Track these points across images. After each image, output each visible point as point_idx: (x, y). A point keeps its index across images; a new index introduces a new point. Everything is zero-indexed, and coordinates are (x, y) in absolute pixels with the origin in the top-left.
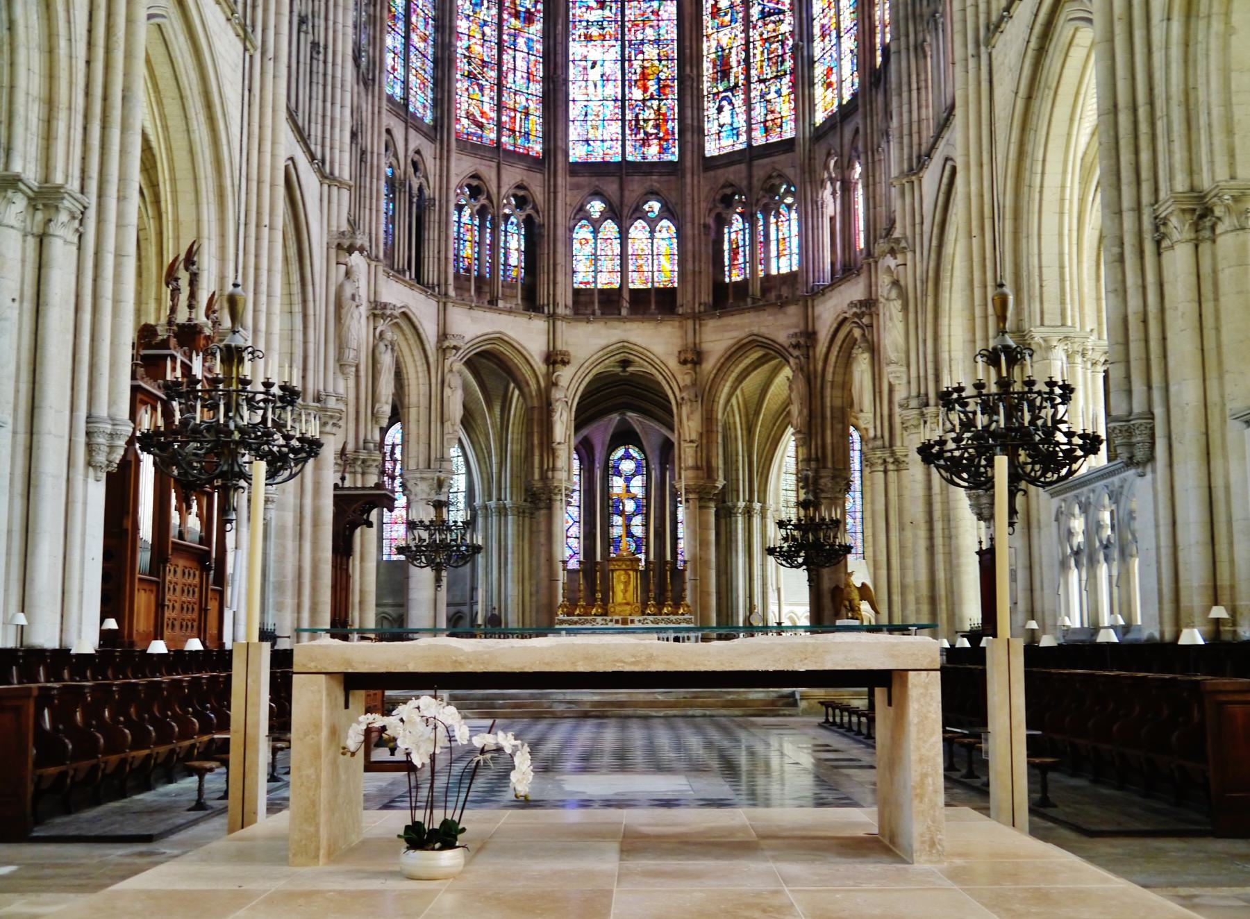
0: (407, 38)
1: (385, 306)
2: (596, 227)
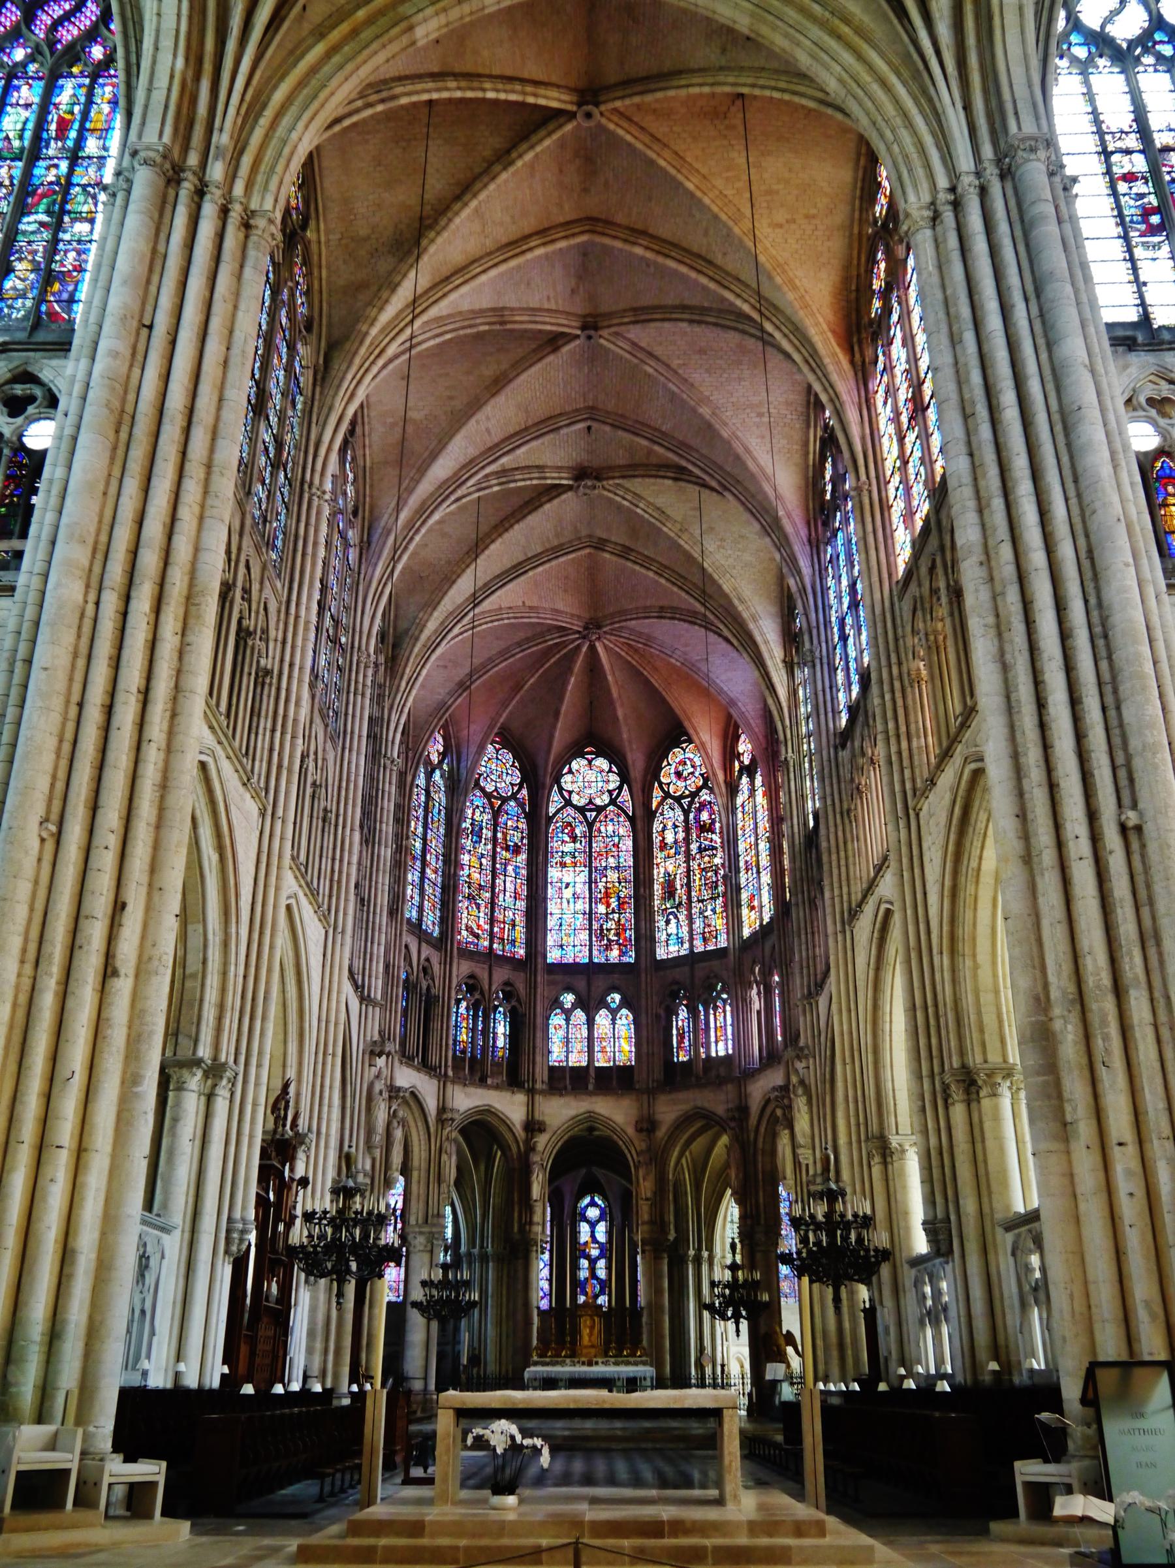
0: (423, 872)
1: (399, 1089)
2: (568, 1014)
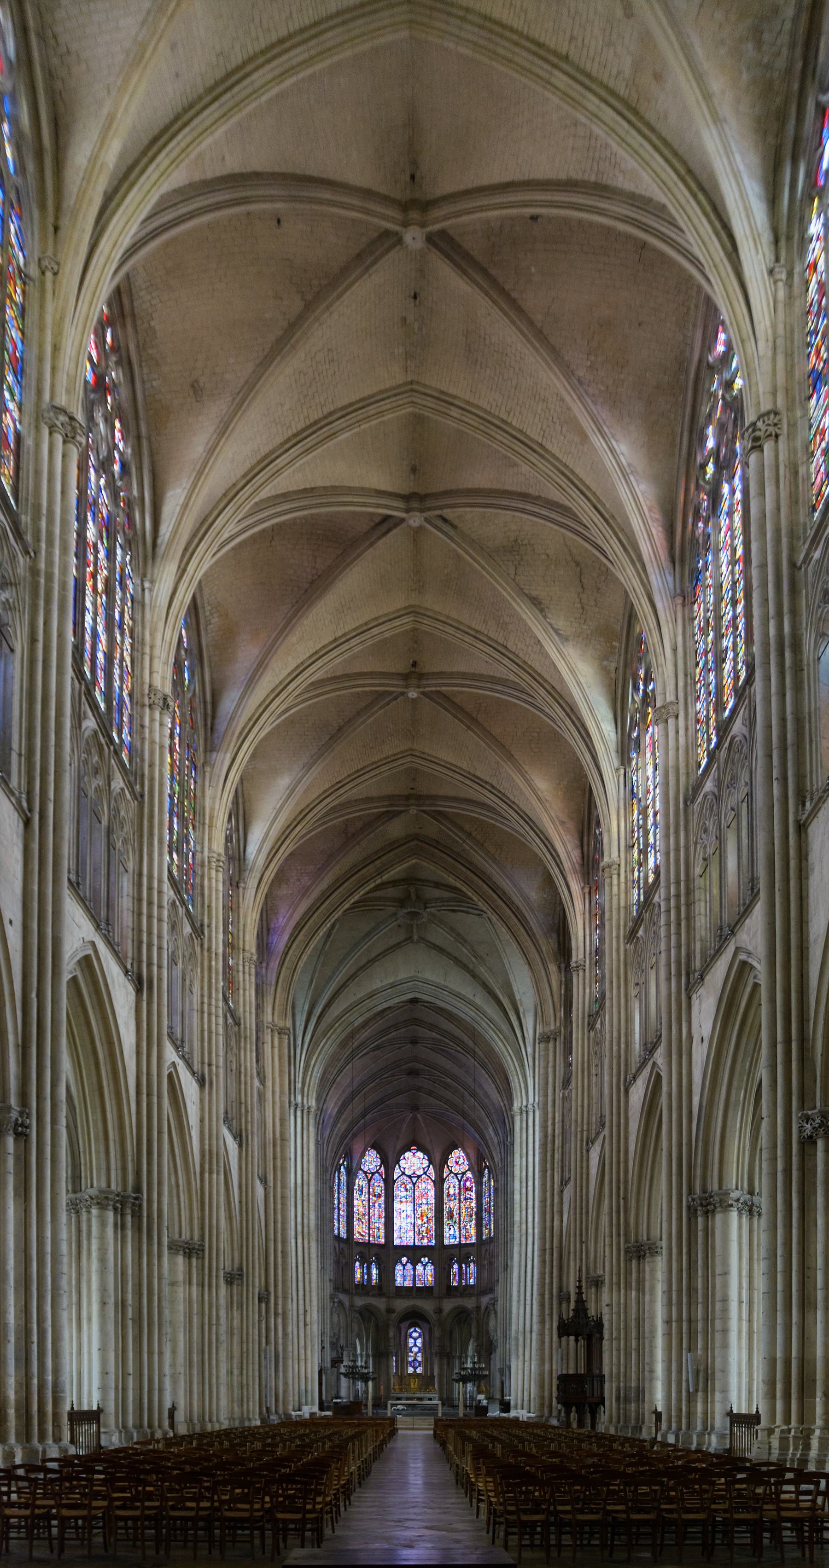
2: (404, 1266)
